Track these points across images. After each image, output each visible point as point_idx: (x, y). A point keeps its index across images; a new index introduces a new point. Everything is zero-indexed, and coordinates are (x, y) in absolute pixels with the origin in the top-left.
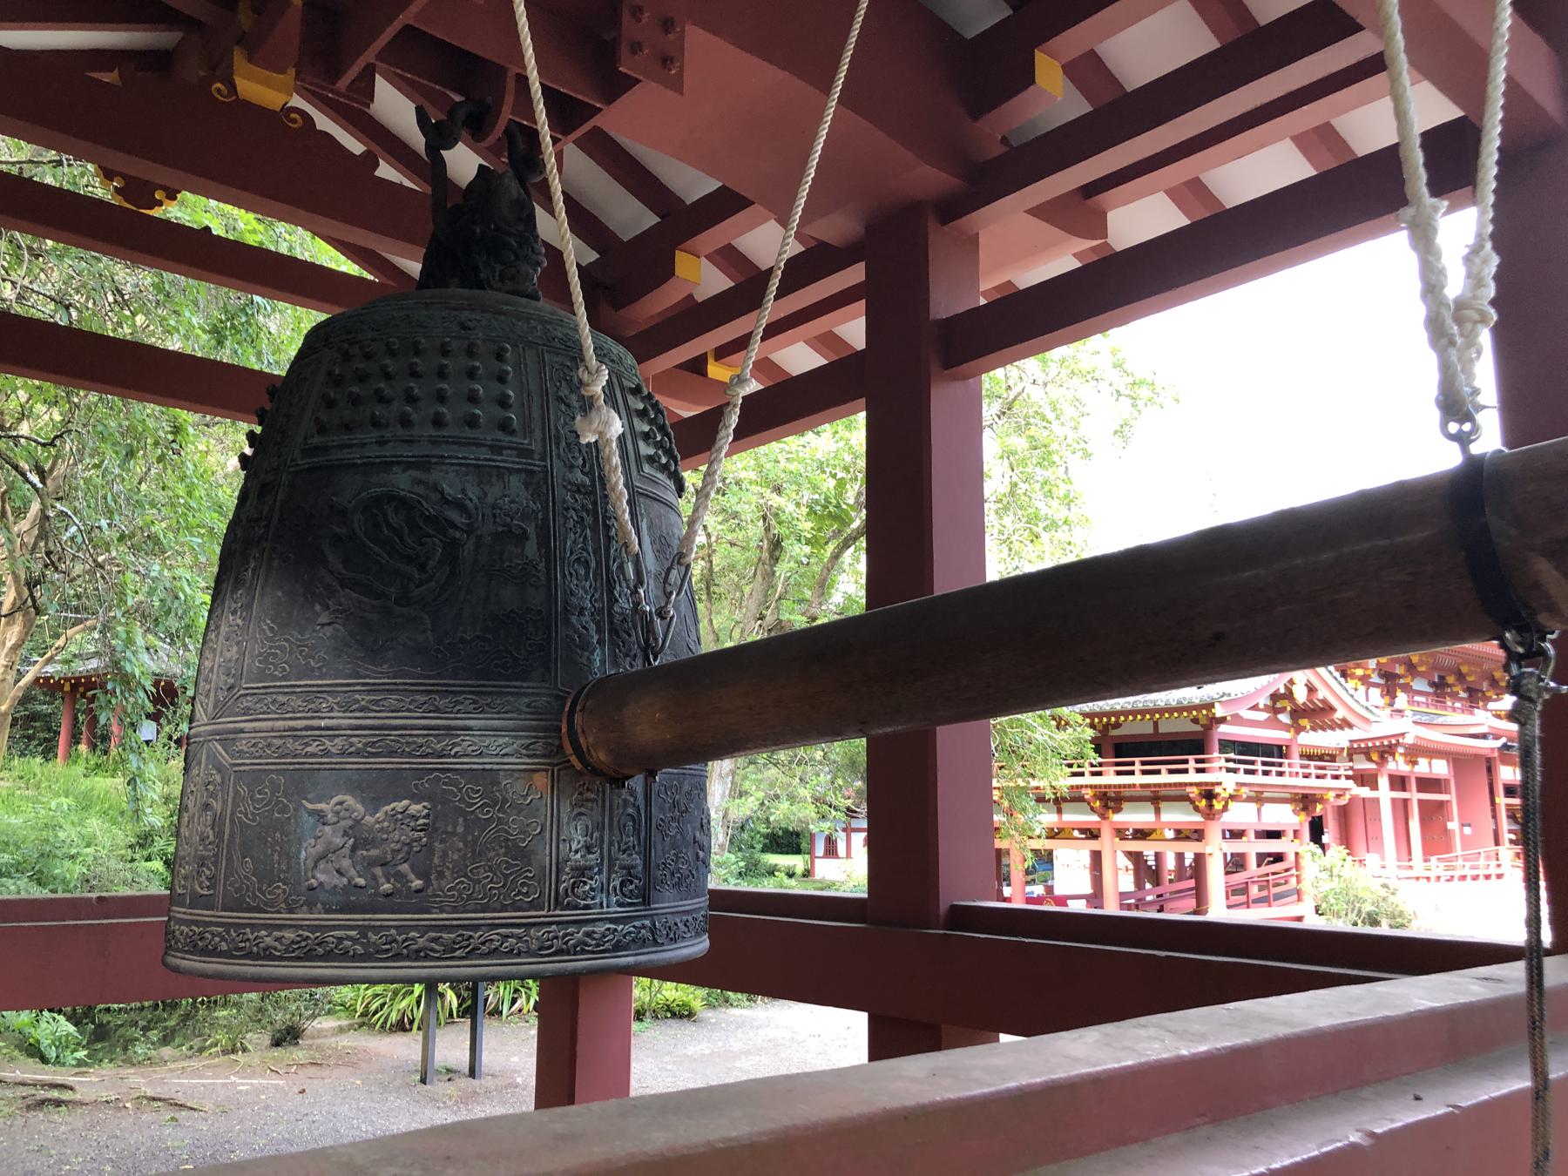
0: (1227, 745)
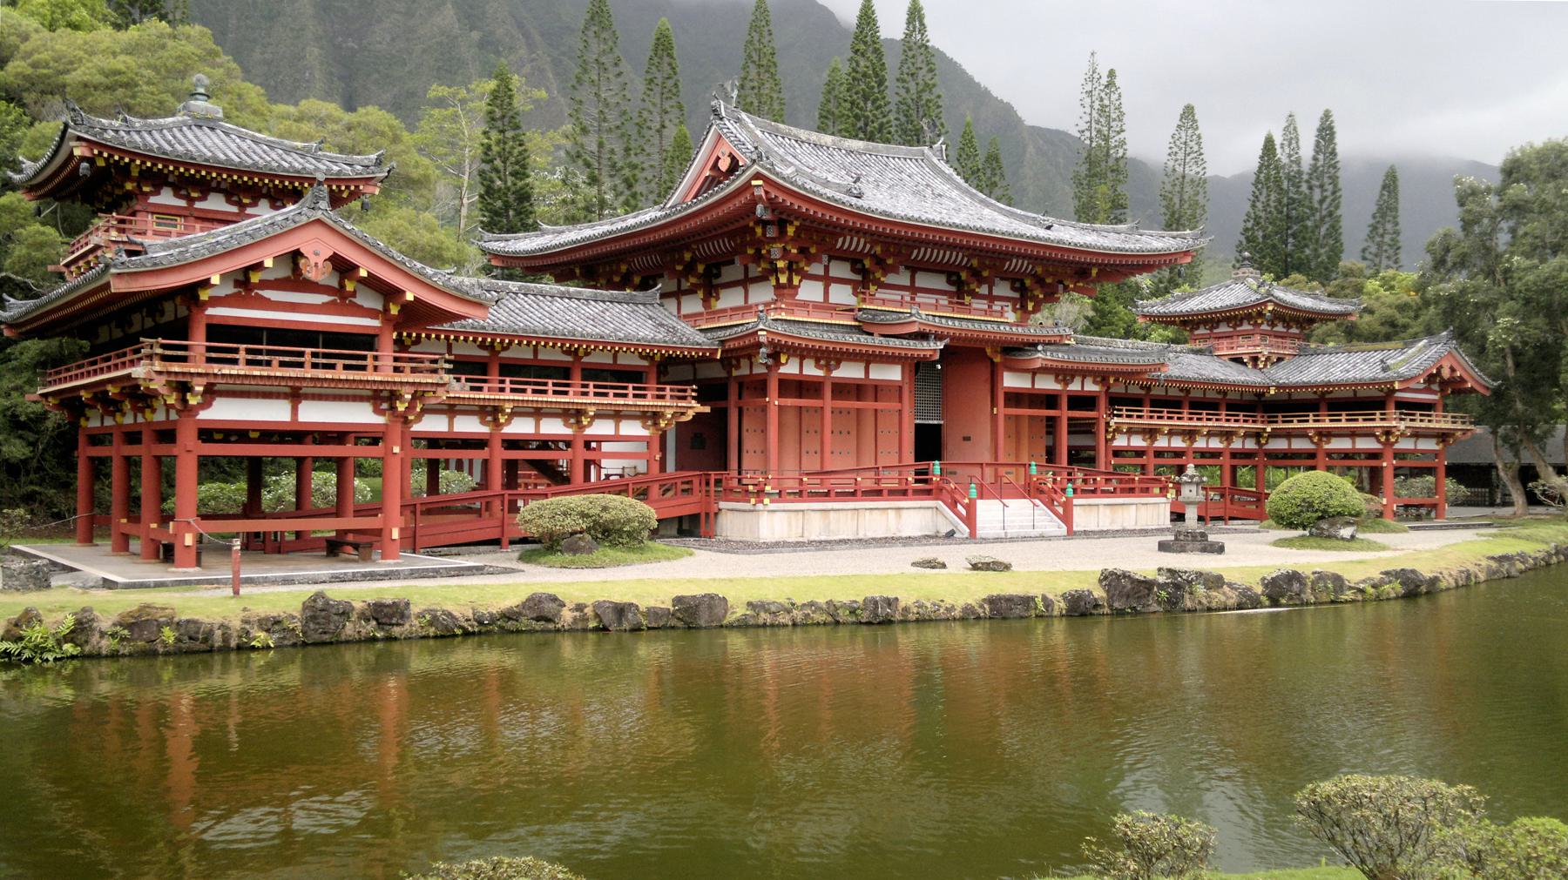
0: (1400, 405)
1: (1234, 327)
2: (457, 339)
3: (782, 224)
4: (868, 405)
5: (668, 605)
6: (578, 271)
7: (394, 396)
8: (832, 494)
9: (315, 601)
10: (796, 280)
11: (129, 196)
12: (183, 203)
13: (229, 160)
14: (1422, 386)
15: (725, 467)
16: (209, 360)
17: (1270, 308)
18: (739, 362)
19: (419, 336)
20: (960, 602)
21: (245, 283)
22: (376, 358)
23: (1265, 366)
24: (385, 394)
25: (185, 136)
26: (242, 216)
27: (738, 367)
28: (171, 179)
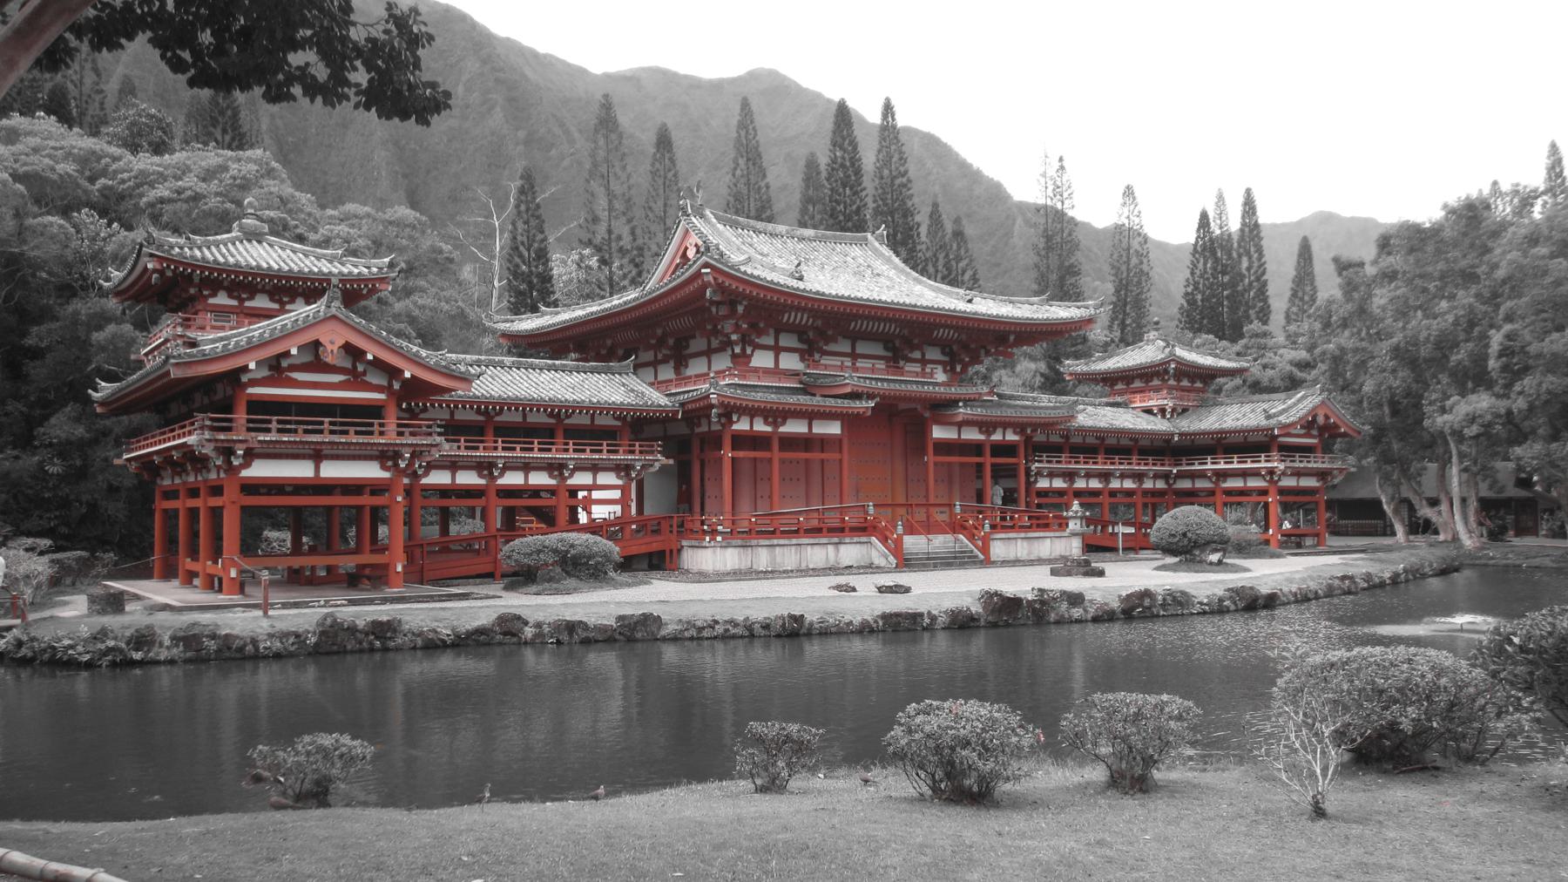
1: (1147, 382)
2: (456, 407)
3: (733, 304)
4: (816, 456)
5: (612, 622)
6: (571, 346)
7: (397, 456)
8: (778, 532)
9: (325, 619)
10: (749, 351)
11: (192, 299)
12: (235, 303)
13: (270, 268)
14: (1303, 432)
15: (691, 510)
16: (249, 430)
17: (1173, 366)
18: (700, 422)
19: (424, 405)
20: (857, 620)
21: (277, 369)
22: (381, 425)
23: (1172, 416)
24: (390, 454)
25: (237, 249)
26: (283, 311)
27: (699, 425)
28: (226, 284)
